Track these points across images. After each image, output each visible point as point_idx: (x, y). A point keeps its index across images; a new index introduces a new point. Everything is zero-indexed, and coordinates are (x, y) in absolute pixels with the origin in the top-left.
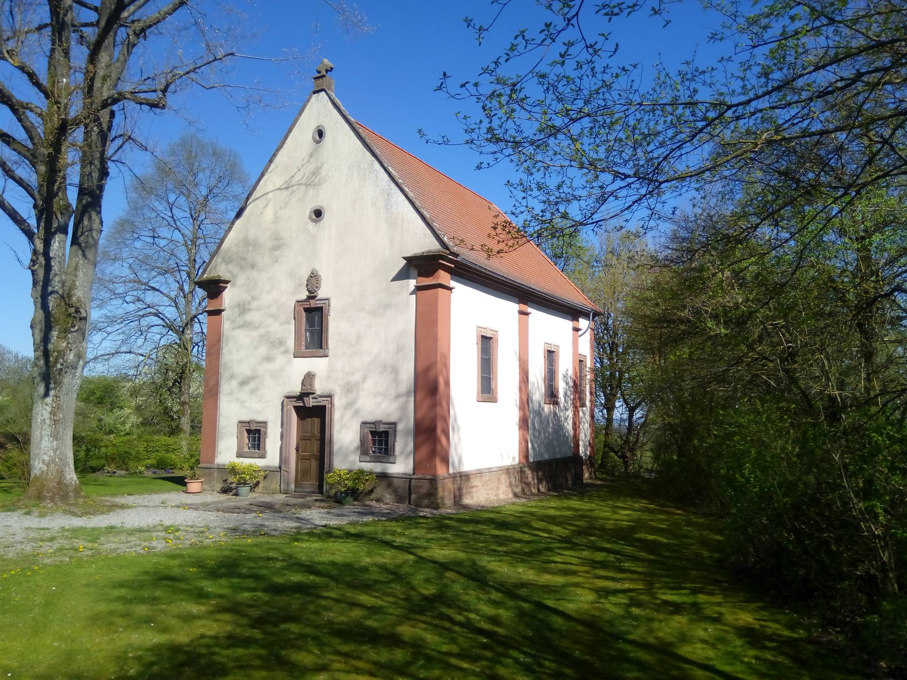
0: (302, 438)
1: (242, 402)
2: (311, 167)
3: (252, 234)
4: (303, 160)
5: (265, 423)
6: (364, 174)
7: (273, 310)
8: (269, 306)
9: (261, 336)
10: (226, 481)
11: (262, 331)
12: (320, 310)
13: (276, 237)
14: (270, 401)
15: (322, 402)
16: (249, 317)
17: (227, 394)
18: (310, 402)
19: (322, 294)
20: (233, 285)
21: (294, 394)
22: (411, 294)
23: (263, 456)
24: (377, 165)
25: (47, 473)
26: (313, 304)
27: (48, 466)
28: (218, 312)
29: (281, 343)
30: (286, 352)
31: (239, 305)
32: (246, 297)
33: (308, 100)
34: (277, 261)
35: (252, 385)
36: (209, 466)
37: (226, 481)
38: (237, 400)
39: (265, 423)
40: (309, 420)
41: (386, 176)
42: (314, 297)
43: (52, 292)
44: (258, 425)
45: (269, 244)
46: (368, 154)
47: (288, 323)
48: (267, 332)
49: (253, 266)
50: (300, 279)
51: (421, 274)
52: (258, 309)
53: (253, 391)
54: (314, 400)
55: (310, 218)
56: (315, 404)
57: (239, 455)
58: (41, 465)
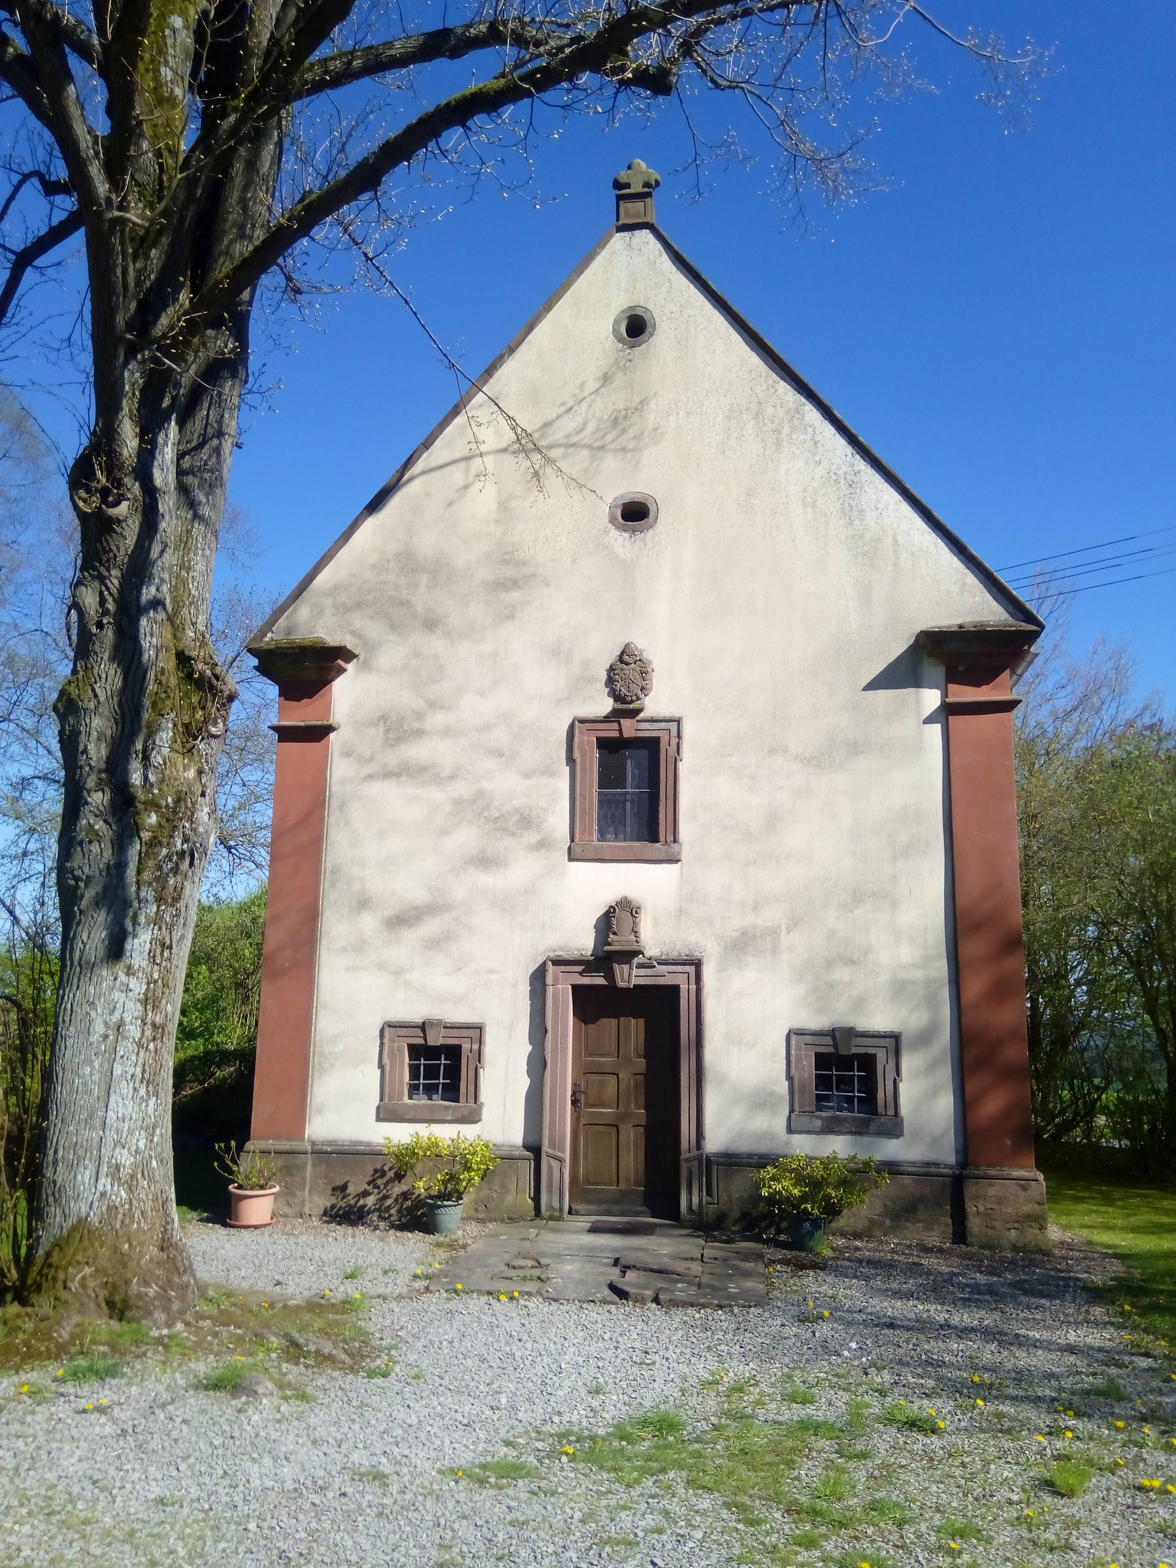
0: (587, 1071)
1: (398, 973)
2: (615, 400)
3: (426, 543)
4: (582, 386)
5: (480, 1028)
6: (777, 431)
7: (500, 736)
8: (486, 727)
9: (459, 803)
10: (344, 1188)
11: (462, 789)
12: (651, 746)
13: (507, 557)
14: (491, 971)
15: (667, 976)
16: (417, 751)
17: (344, 949)
18: (629, 976)
19: (655, 705)
20: (367, 667)
21: (574, 955)
22: (928, 720)
23: (472, 1118)
24: (812, 414)
25: (130, 1214)
26: (629, 728)
27: (131, 1188)
28: (319, 733)
29: (526, 821)
30: (544, 844)
31: (384, 718)
32: (405, 699)
33: (602, 244)
34: (510, 617)
35: (431, 927)
36: (285, 1145)
37: (344, 1188)
38: (380, 966)
39: (390, 1027)
40: (608, 1025)
41: (841, 443)
42: (633, 713)
43: (157, 603)
44: (455, 1032)
45: (485, 573)
46: (785, 390)
47: (549, 772)
48: (480, 793)
49: (431, 624)
50: (585, 665)
51: (953, 677)
52: (447, 732)
53: (435, 944)
54: (643, 972)
55: (612, 520)
56: (642, 981)
57: (386, 1113)
58: (104, 1182)
